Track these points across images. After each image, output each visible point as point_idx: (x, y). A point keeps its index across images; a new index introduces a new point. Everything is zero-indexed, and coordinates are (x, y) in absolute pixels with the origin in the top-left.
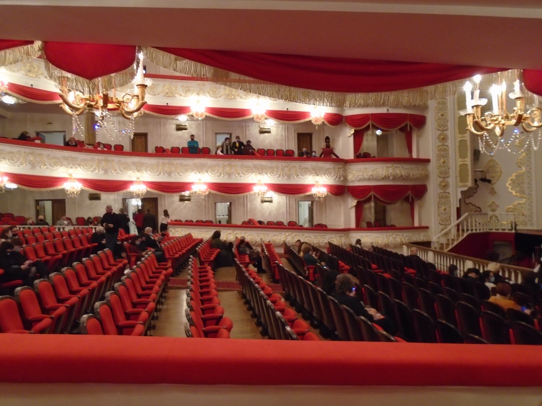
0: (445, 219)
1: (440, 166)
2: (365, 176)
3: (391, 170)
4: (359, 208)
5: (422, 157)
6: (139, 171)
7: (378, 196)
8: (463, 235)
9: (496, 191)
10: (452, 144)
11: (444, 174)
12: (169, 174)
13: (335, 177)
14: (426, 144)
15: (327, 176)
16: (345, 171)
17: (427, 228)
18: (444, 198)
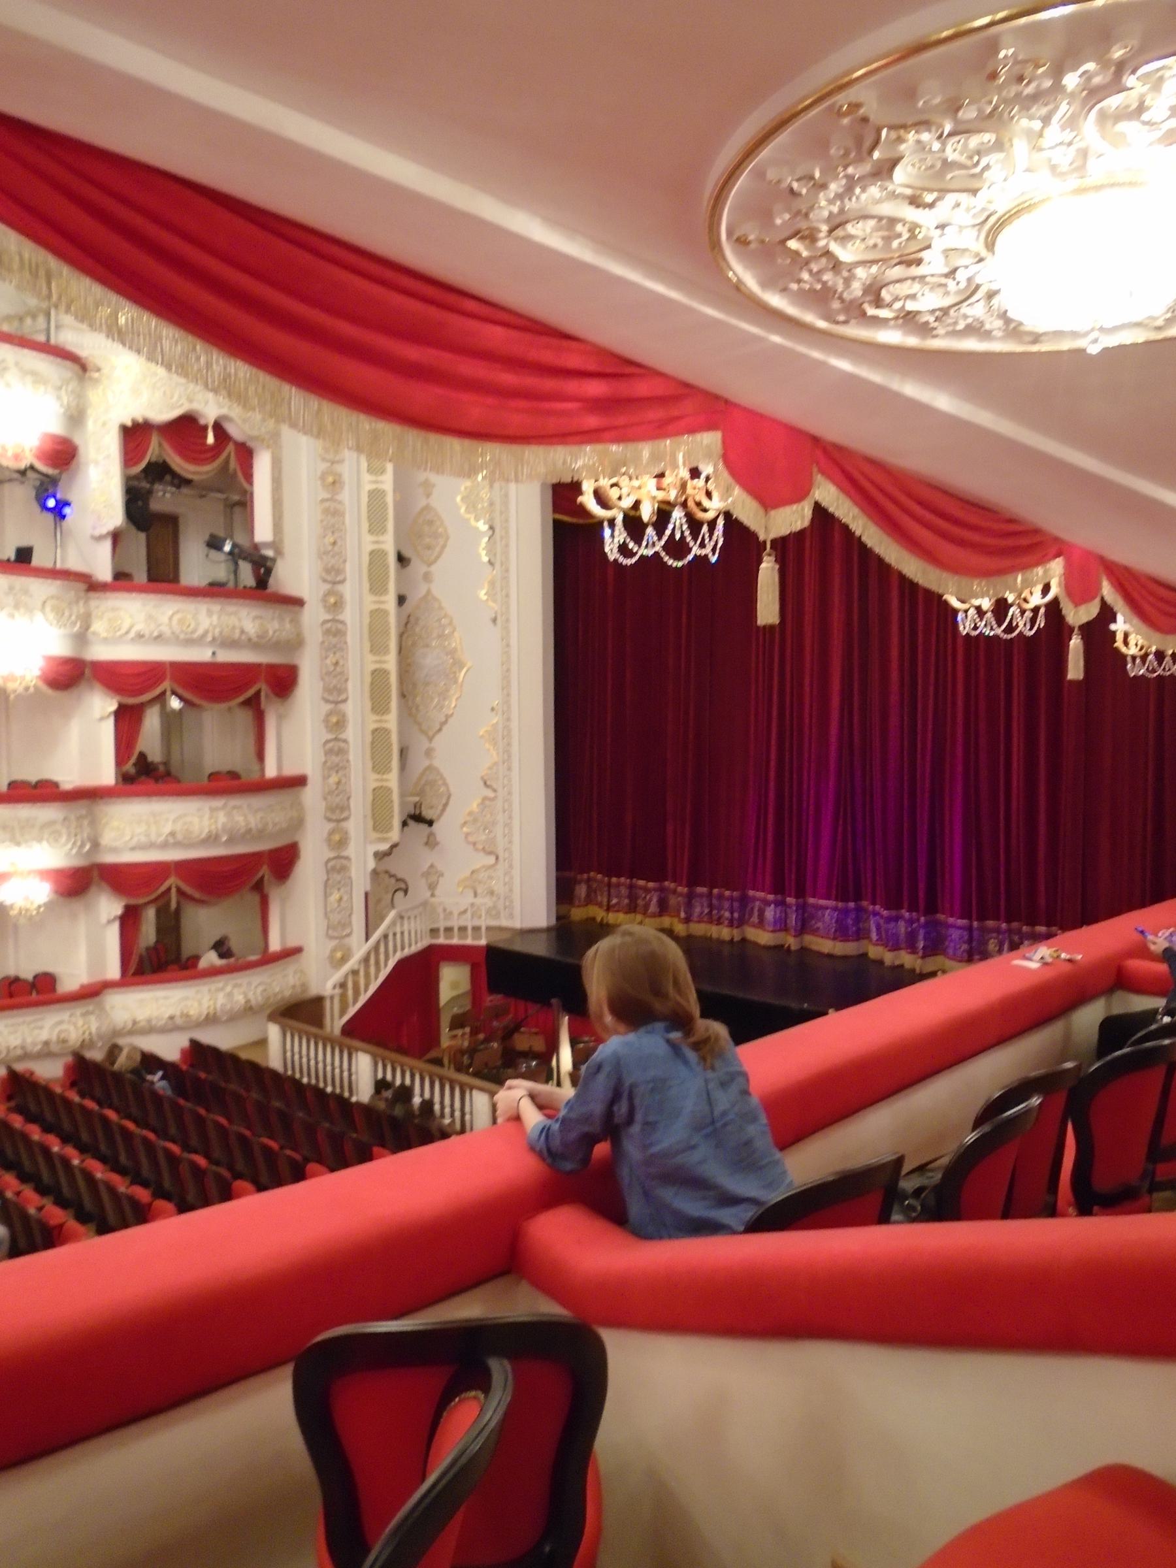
0: (339, 922)
1: (330, 793)
2: (153, 838)
3: (222, 818)
4: (129, 920)
5: (290, 771)
7: (188, 890)
8: (386, 965)
9: (439, 838)
10: (356, 736)
11: (338, 812)
13: (69, 846)
14: (296, 739)
15: (45, 843)
16: (93, 823)
17: (298, 951)
18: (339, 872)
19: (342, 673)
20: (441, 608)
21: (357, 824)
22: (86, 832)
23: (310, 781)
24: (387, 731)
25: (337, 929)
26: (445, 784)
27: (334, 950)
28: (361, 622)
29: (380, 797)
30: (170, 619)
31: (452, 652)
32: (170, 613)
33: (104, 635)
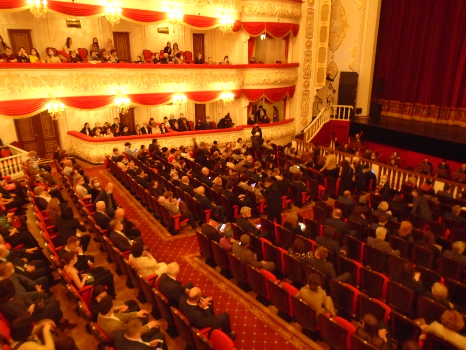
1: (306, 69)
2: (259, 81)
5: (295, 61)
6: (51, 86)
10: (314, 50)
11: (307, 76)
12: (86, 88)
16: (243, 76)
19: (312, 28)
20: (341, 5)
21: (313, 80)
22: (241, 80)
23: (300, 65)
24: (324, 48)
25: (304, 115)
26: (337, 68)
27: (303, 120)
28: (319, 9)
29: (320, 70)
30: (267, 6)
31: (343, 22)
32: (267, 5)
33: (247, 13)
